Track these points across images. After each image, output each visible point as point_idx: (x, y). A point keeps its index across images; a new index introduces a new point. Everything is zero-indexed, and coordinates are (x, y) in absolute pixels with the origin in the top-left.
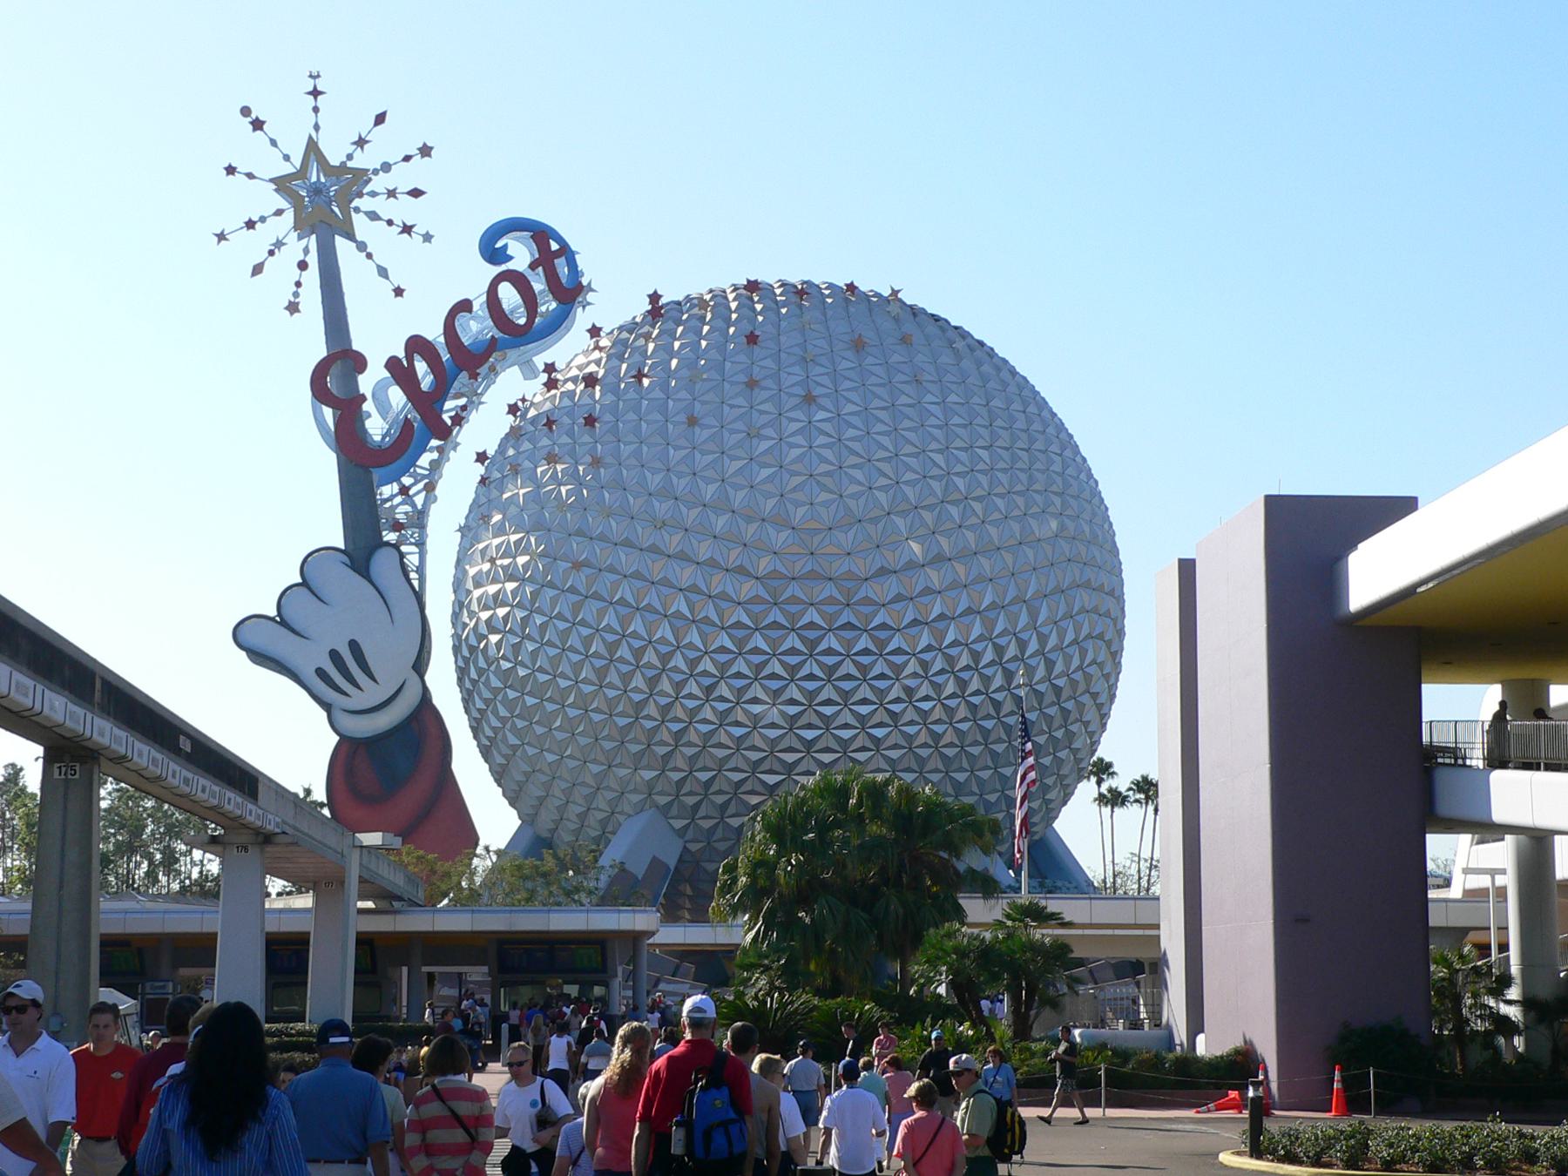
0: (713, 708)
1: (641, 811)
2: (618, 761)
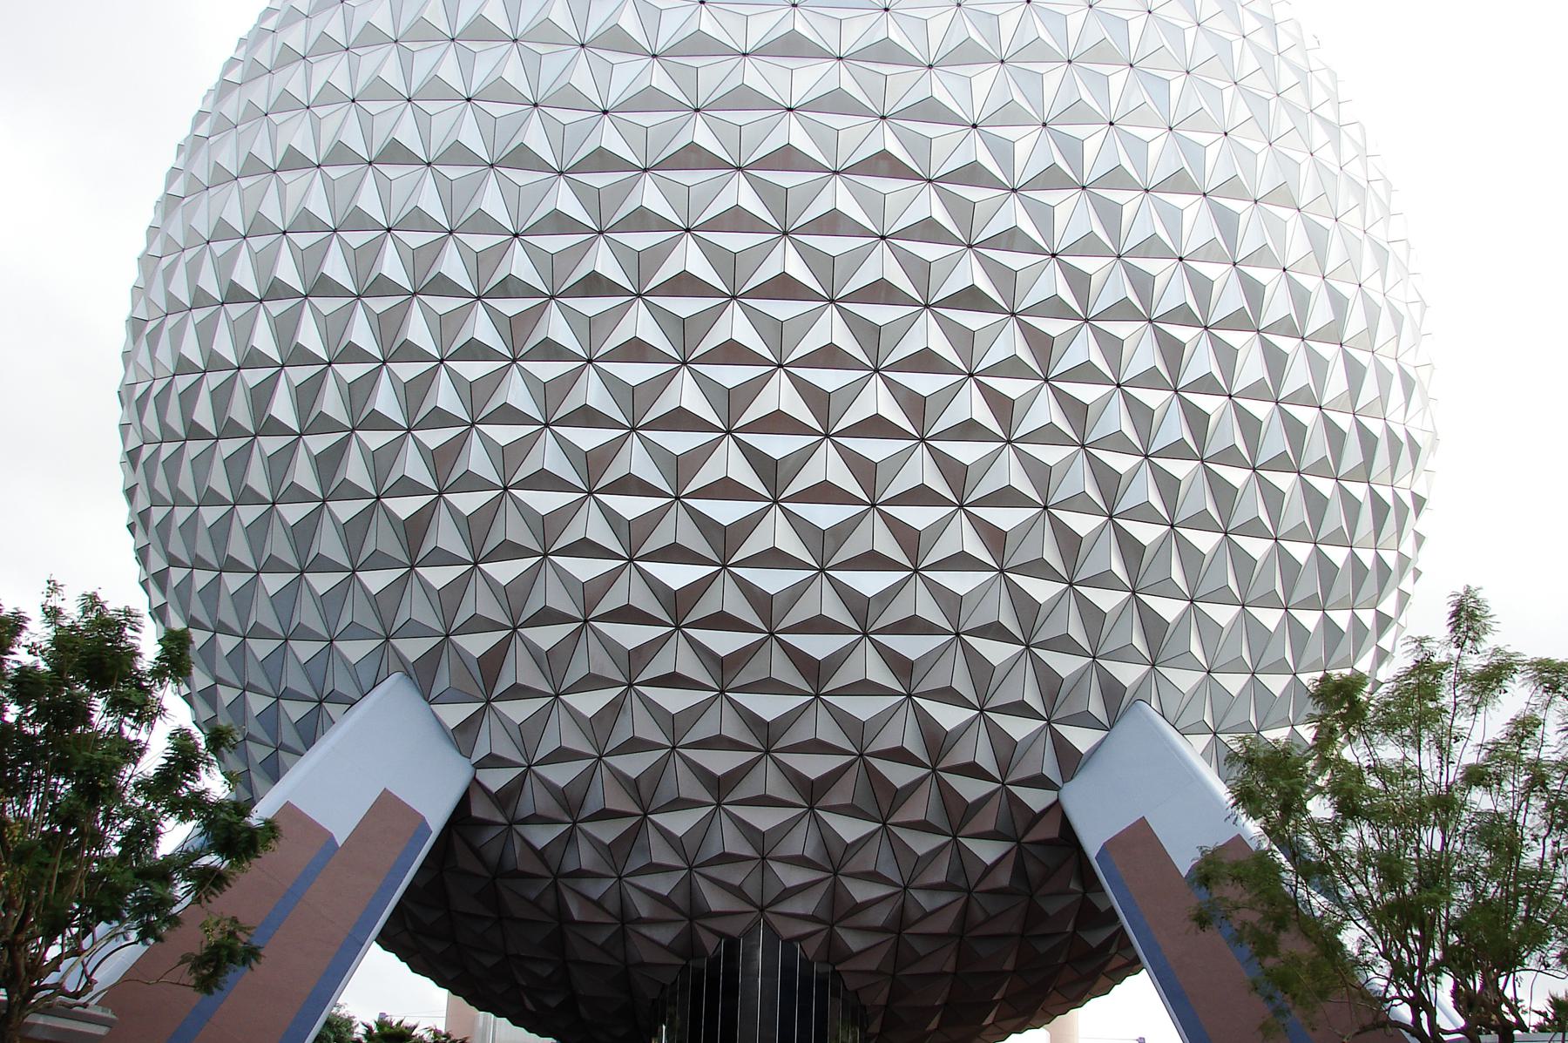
1: (374, 687)
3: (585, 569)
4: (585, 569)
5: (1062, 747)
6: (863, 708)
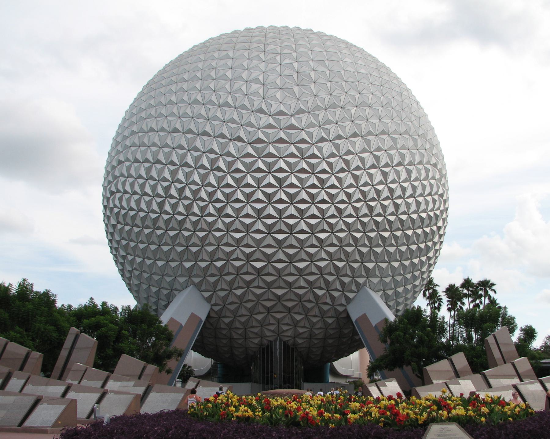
0: (223, 222)
1: (186, 287)
2: (171, 258)
3: (238, 264)
4: (238, 264)
5: (347, 298)
6: (301, 292)
